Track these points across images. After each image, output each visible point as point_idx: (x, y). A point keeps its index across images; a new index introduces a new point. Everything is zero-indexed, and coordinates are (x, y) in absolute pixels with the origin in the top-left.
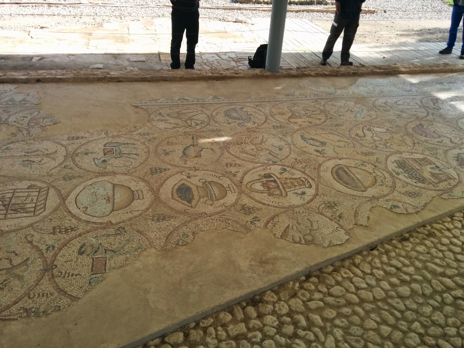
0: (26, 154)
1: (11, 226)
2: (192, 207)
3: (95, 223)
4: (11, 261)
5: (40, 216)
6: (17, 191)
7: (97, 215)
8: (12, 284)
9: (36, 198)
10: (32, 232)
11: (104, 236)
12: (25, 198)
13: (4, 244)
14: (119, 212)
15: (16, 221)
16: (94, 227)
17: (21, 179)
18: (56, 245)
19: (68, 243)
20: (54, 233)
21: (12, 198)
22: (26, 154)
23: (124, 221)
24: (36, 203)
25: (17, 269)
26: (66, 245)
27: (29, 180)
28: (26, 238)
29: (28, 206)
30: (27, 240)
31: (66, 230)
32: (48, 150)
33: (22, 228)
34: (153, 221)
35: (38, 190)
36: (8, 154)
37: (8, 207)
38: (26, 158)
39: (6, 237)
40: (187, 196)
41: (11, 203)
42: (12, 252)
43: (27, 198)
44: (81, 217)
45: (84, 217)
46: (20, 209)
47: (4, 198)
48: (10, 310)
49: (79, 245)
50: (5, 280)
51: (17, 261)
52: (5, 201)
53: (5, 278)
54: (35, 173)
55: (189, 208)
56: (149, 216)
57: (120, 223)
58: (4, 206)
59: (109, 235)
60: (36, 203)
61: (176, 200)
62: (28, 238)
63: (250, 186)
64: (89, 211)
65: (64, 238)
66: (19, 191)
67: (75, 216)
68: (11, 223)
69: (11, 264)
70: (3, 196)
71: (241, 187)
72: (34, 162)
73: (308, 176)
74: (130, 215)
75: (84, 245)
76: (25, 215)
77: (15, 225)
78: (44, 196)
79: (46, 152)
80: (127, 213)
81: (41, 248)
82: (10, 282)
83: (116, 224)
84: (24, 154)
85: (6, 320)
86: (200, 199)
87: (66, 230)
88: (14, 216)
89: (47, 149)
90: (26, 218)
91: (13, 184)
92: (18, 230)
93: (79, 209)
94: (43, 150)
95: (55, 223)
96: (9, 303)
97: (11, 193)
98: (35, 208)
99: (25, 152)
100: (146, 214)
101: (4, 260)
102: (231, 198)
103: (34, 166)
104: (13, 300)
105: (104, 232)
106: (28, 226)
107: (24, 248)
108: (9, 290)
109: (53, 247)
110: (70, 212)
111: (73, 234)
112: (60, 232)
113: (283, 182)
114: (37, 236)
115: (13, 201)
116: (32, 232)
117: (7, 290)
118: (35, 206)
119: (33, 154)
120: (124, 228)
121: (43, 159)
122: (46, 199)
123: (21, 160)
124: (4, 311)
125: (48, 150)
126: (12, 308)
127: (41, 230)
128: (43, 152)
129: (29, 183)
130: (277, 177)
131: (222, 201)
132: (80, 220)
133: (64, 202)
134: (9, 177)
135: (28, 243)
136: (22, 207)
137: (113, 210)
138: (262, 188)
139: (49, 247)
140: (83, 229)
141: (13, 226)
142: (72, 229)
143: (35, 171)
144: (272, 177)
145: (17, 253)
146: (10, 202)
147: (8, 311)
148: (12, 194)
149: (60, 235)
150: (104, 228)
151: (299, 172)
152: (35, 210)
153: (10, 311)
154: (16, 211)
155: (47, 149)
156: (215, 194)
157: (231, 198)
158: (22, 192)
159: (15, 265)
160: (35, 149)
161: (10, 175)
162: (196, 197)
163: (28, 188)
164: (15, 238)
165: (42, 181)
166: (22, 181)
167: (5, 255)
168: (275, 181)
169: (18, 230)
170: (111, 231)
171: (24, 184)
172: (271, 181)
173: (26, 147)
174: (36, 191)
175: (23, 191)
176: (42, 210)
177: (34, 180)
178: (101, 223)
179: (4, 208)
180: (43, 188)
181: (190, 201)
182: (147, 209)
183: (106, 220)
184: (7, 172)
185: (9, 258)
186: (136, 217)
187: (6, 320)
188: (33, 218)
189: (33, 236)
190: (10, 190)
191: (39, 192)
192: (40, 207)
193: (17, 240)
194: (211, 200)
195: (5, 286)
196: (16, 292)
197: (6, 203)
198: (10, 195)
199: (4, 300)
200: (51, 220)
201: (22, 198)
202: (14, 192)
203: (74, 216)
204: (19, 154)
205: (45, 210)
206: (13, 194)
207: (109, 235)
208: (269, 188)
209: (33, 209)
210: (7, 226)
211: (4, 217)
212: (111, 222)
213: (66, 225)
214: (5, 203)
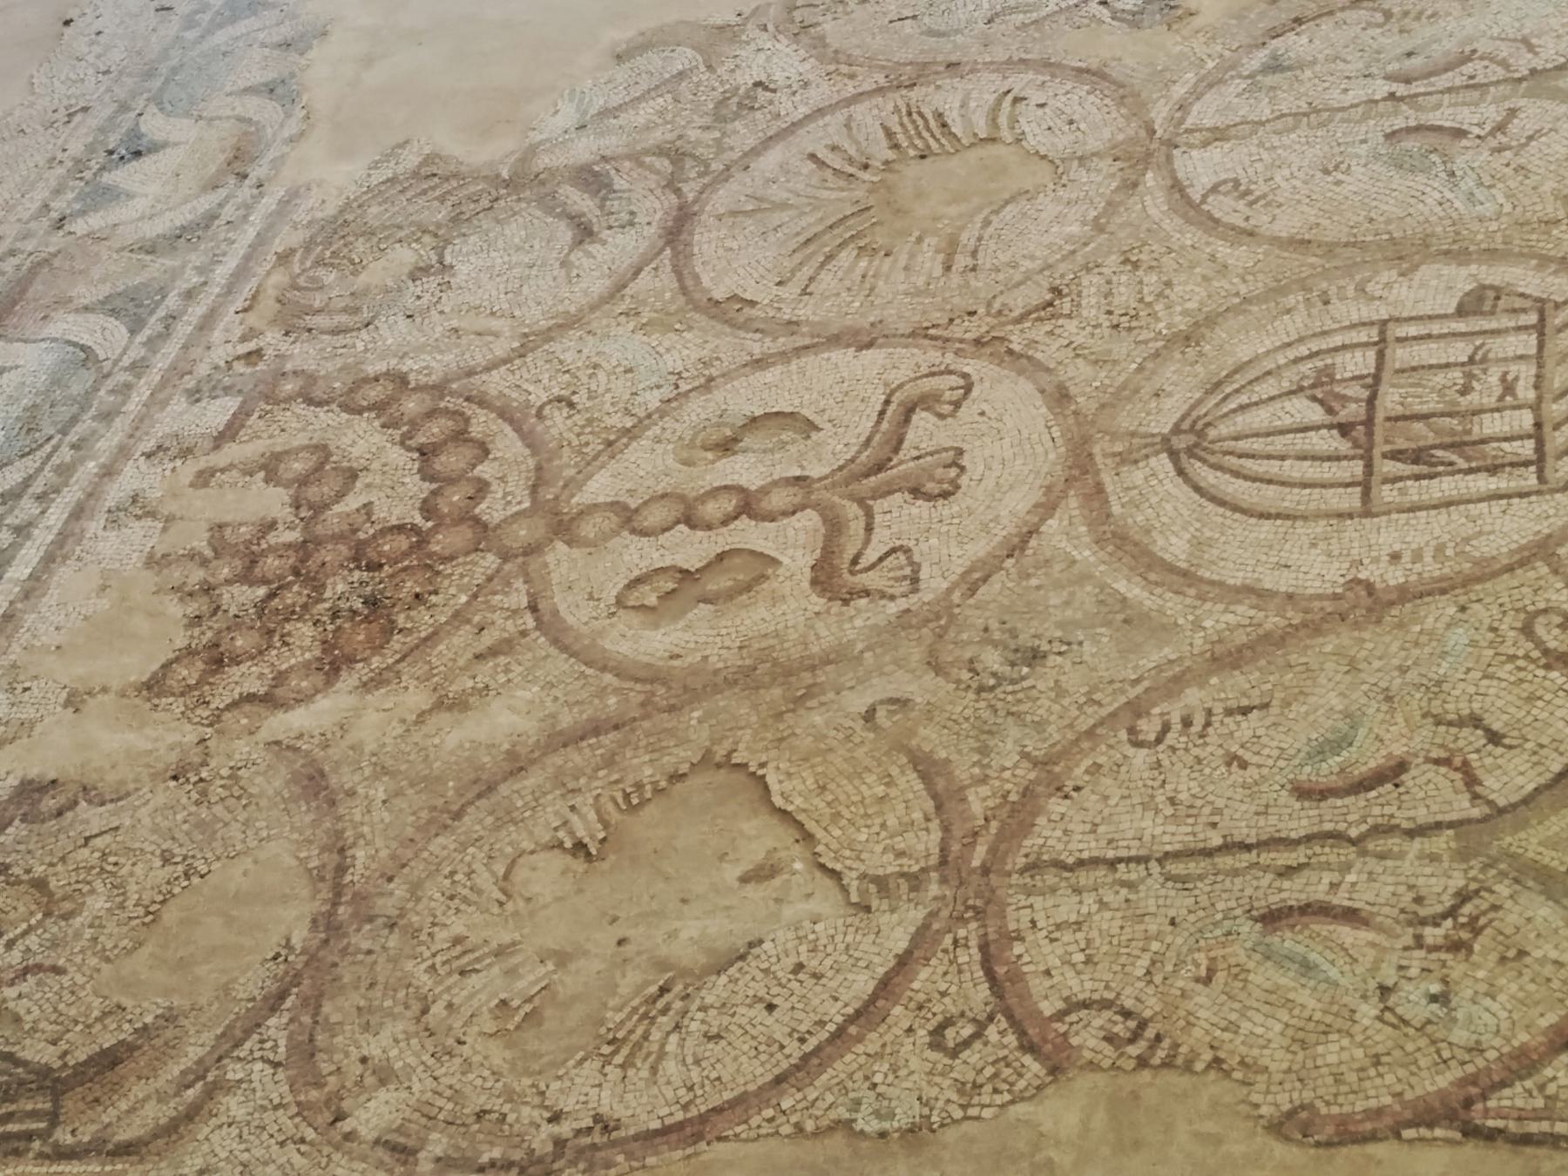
0: (1401, 89)
1: (1417, 556)
4: (1471, 781)
6: (1402, 331)
8: (1513, 919)
9: (1527, 372)
12: (1457, 375)
13: (1403, 670)
15: (1439, 525)
17: (1406, 253)
21: (1377, 377)
22: (1401, 89)
24: (1536, 407)
25: (1524, 824)
27: (1459, 255)
28: (1527, 630)
29: (1491, 425)
30: (1539, 644)
32: (1531, 48)
33: (1486, 571)
35: (1533, 318)
36: (1287, 103)
37: (1370, 434)
38: (1406, 117)
39: (1401, 625)
41: (1380, 416)
42: (1460, 723)
43: (1470, 376)
47: (1333, 380)
48: (1538, 1078)
50: (1463, 897)
51: (1509, 777)
53: (1458, 881)
54: (1488, 209)
58: (1344, 429)
60: (1536, 407)
62: (1540, 630)
66: (1413, 330)
68: (1416, 539)
69: (1476, 797)
70: (1319, 372)
72: (1460, 133)
76: (1484, 483)
77: (1440, 549)
79: (1524, 63)
82: (1495, 908)
84: (1382, 88)
85: (1526, 1140)
88: (1416, 491)
89: (1525, 41)
90: (1498, 506)
91: (1361, 289)
92: (1468, 581)
94: (1504, 51)
96: (1523, 1037)
97: (1366, 345)
99: (1387, 78)
101: (1431, 772)
103: (1467, 158)
104: (1544, 1023)
106: (1524, 558)
107: (1531, 698)
108: (1503, 959)
115: (1391, 399)
117: (1493, 957)
118: (1538, 425)
119: (1442, 81)
121: (1513, 112)
123: (1374, 129)
124: (1503, 1084)
125: (1531, 48)
126: (1548, 1072)
128: (1504, 64)
129: (1463, 278)
134: (1330, 249)
135: (1548, 667)
136: (1453, 433)
141: (1428, 559)
143: (1480, 194)
145: (1496, 726)
146: (1371, 402)
147: (1528, 1084)
148: (1371, 354)
153: (1542, 1087)
155: (1525, 41)
158: (1429, 336)
159: (1502, 802)
160: (1450, 46)
161: (1334, 231)
163: (1461, 312)
164: (1460, 636)
165: (1544, 261)
166: (1415, 267)
167: (1424, 739)
169: (1468, 581)
171: (1437, 288)
173: (1391, 43)
174: (1519, 329)
175: (1436, 328)
177: (1491, 255)
179: (1344, 446)
180: (1557, 306)
184: (1312, 214)
185: (1457, 761)
187: (1526, 1140)
188: (1541, 505)
190: (1353, 326)
191: (1540, 328)
193: (1473, 643)
195: (1474, 927)
196: (1548, 970)
197: (1352, 411)
198: (1360, 363)
199: (1486, 1017)
201: (1439, 379)
202: (1383, 340)
204: (1357, 94)
206: (1381, 356)
209: (1530, 445)
211: (1357, 504)
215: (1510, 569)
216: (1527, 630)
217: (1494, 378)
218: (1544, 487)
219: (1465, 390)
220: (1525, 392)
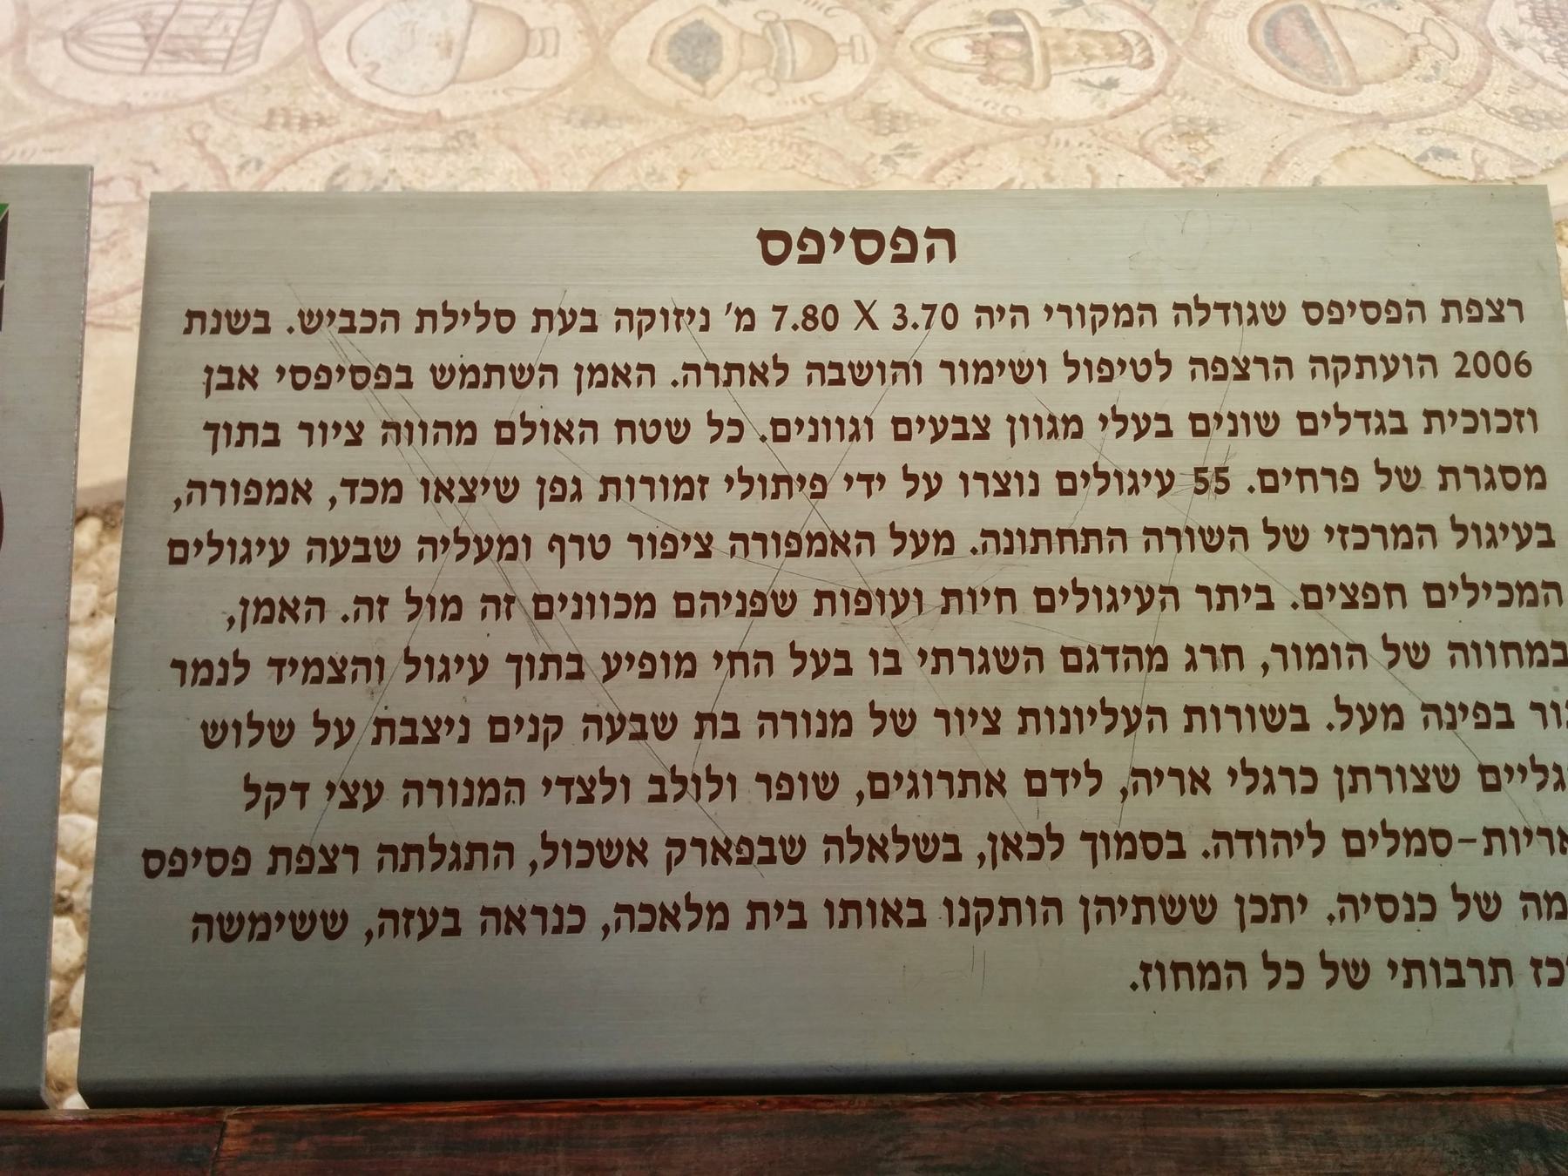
2: (704, 95)
3: (392, 112)
4: (139, 185)
5: (236, 76)
7: (402, 89)
9: (235, 25)
10: (209, 117)
11: (408, 149)
14: (471, 87)
16: (384, 123)
18: (269, 161)
19: (301, 157)
20: (268, 126)
23: (478, 116)
26: (295, 162)
28: (189, 130)
31: (305, 123)
33: (183, 104)
34: (568, 122)
40: (700, 60)
41: (167, 31)
44: (354, 91)
45: (364, 91)
46: (190, 51)
49: (333, 166)
50: (115, 232)
52: (152, 25)
53: (116, 226)
55: (694, 98)
56: (559, 107)
57: (464, 118)
58: (147, 38)
59: (423, 150)
60: (234, 40)
61: (660, 70)
63: (927, 49)
64: (380, 77)
65: (294, 142)
67: (337, 85)
71: (894, 46)
73: (1156, 27)
74: (501, 100)
75: (345, 168)
76: (199, 68)
78: (262, 23)
80: (495, 92)
81: (224, 161)
83: (455, 120)
86: (738, 72)
87: (305, 123)
88: (167, 67)
93: (355, 66)
95: (279, 99)
98: (230, 51)
100: (550, 100)
102: (845, 78)
105: (412, 139)
109: (259, 164)
110: (325, 74)
111: (324, 133)
112: (287, 125)
113: (1050, 42)
114: (220, 130)
115: (173, 27)
116: (209, 117)
118: (232, 47)
120: (473, 136)
122: (264, 31)
127: (234, 113)
130: (1036, 23)
131: (809, 87)
132: (347, 96)
133: (316, 45)
137: (453, 81)
138: (966, 56)
139: (248, 162)
140: (353, 125)
142: (321, 121)
144: (1017, 21)
146: (164, 28)
149: (284, 132)
150: (416, 128)
151: (1126, 14)
152: (228, 57)
154: (175, 55)
156: (794, 62)
157: (845, 78)
162: (728, 66)
168: (1023, 38)
170: (434, 138)
172: (1009, 36)
176: (249, 60)
178: (410, 114)
181: (701, 78)
182: (560, 87)
183: (425, 106)
186: (517, 107)
189: (209, 126)
192: (244, 51)
194: (774, 79)
195: (114, 245)
198: (165, 10)
200: (268, 89)
203: (335, 86)
205: (256, 60)
207: (423, 150)
208: (990, 57)
210: (146, 94)
212: (438, 113)
213: (308, 109)
214: (150, 31)
215: (193, 104)
216: (189, 130)
217: (221, 25)
218: (224, 72)
219: (208, 28)
220: (233, 32)
